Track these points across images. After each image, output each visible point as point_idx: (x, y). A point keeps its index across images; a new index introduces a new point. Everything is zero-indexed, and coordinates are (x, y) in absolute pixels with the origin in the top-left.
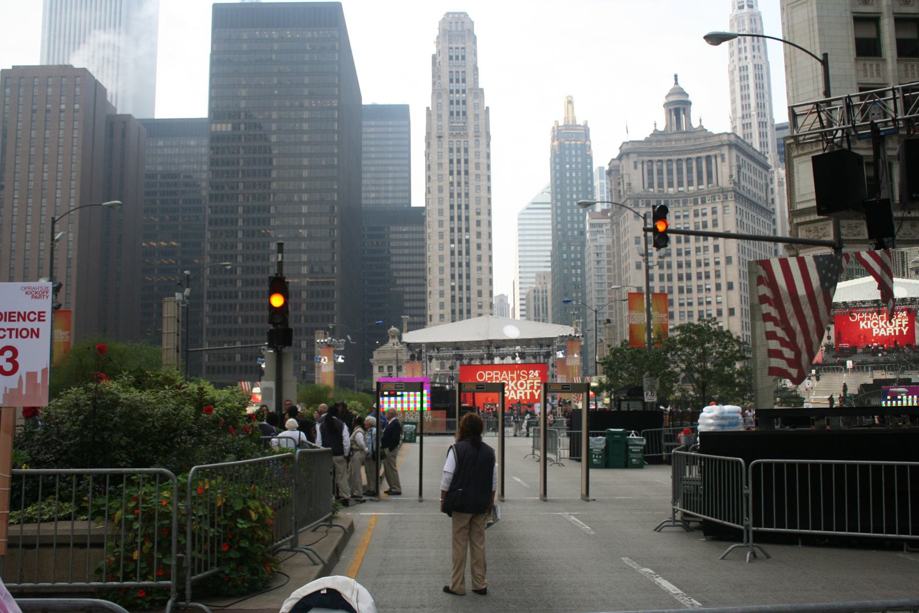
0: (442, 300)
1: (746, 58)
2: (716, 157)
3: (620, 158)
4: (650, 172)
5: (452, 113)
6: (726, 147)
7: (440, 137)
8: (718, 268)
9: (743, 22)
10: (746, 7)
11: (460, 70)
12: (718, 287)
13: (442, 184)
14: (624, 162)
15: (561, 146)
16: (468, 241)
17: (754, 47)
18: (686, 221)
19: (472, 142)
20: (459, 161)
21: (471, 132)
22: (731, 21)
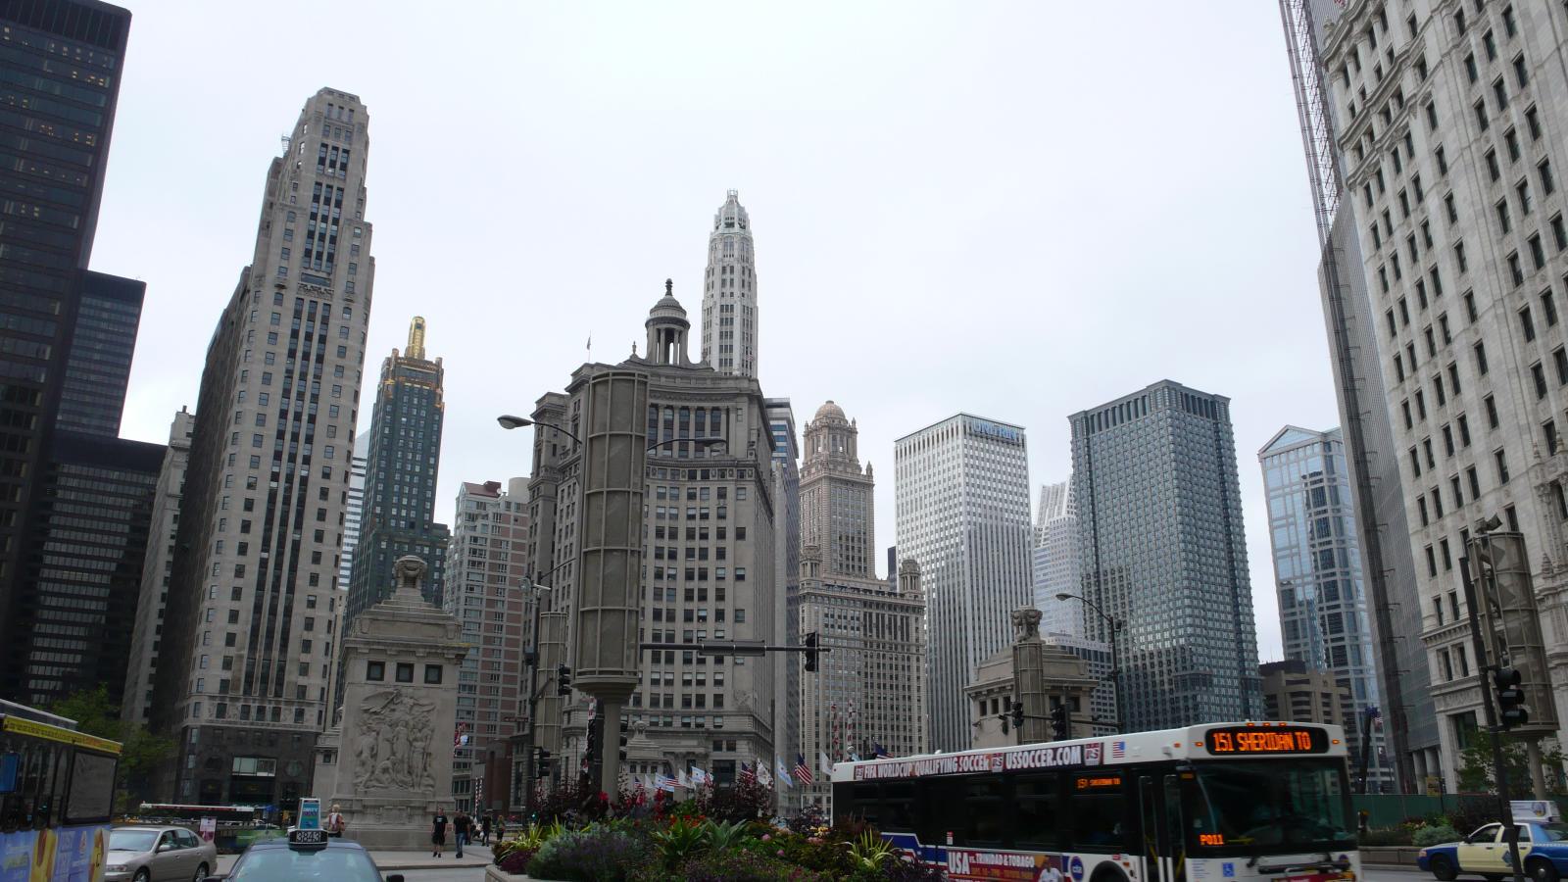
0: (239, 582)
1: (732, 294)
2: (728, 411)
3: (573, 389)
5: (308, 253)
6: (746, 399)
7: (281, 287)
8: (721, 585)
9: (732, 245)
10: (737, 226)
11: (336, 184)
12: (720, 615)
13: (269, 369)
14: (582, 396)
15: (397, 387)
16: (304, 481)
17: (743, 281)
18: (674, 504)
19: (337, 307)
20: (309, 337)
21: (339, 289)
22: (713, 241)
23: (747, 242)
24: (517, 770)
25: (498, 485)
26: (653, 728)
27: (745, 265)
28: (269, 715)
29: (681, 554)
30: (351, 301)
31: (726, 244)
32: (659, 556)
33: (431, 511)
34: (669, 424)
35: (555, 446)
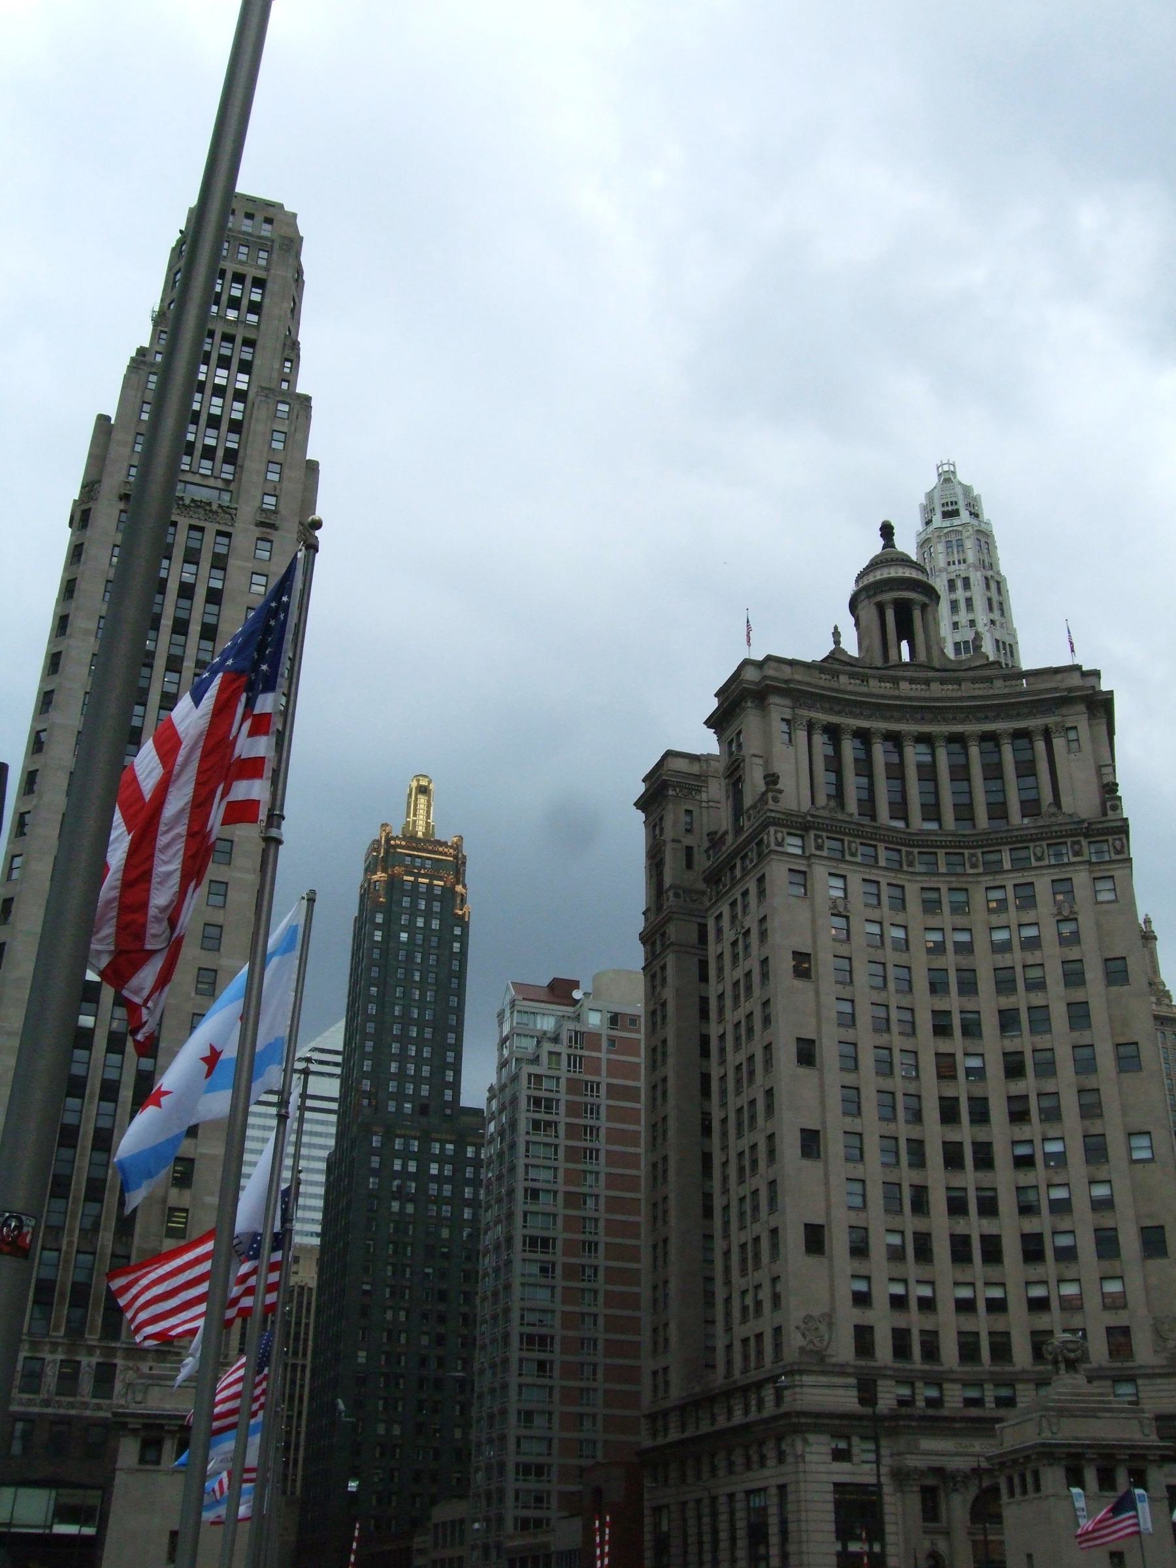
2: (1047, 735)
4: (835, 764)
6: (1082, 708)
9: (960, 545)
15: (393, 884)
17: (990, 600)
18: (961, 921)
23: (985, 539)
24: (657, 1525)
25: (575, 985)
26: (974, 1412)
27: (989, 573)
28: (86, 1384)
29: (990, 1024)
30: (272, 526)
31: (949, 545)
32: (941, 1029)
33: (456, 1086)
34: (928, 773)
35: (689, 850)
